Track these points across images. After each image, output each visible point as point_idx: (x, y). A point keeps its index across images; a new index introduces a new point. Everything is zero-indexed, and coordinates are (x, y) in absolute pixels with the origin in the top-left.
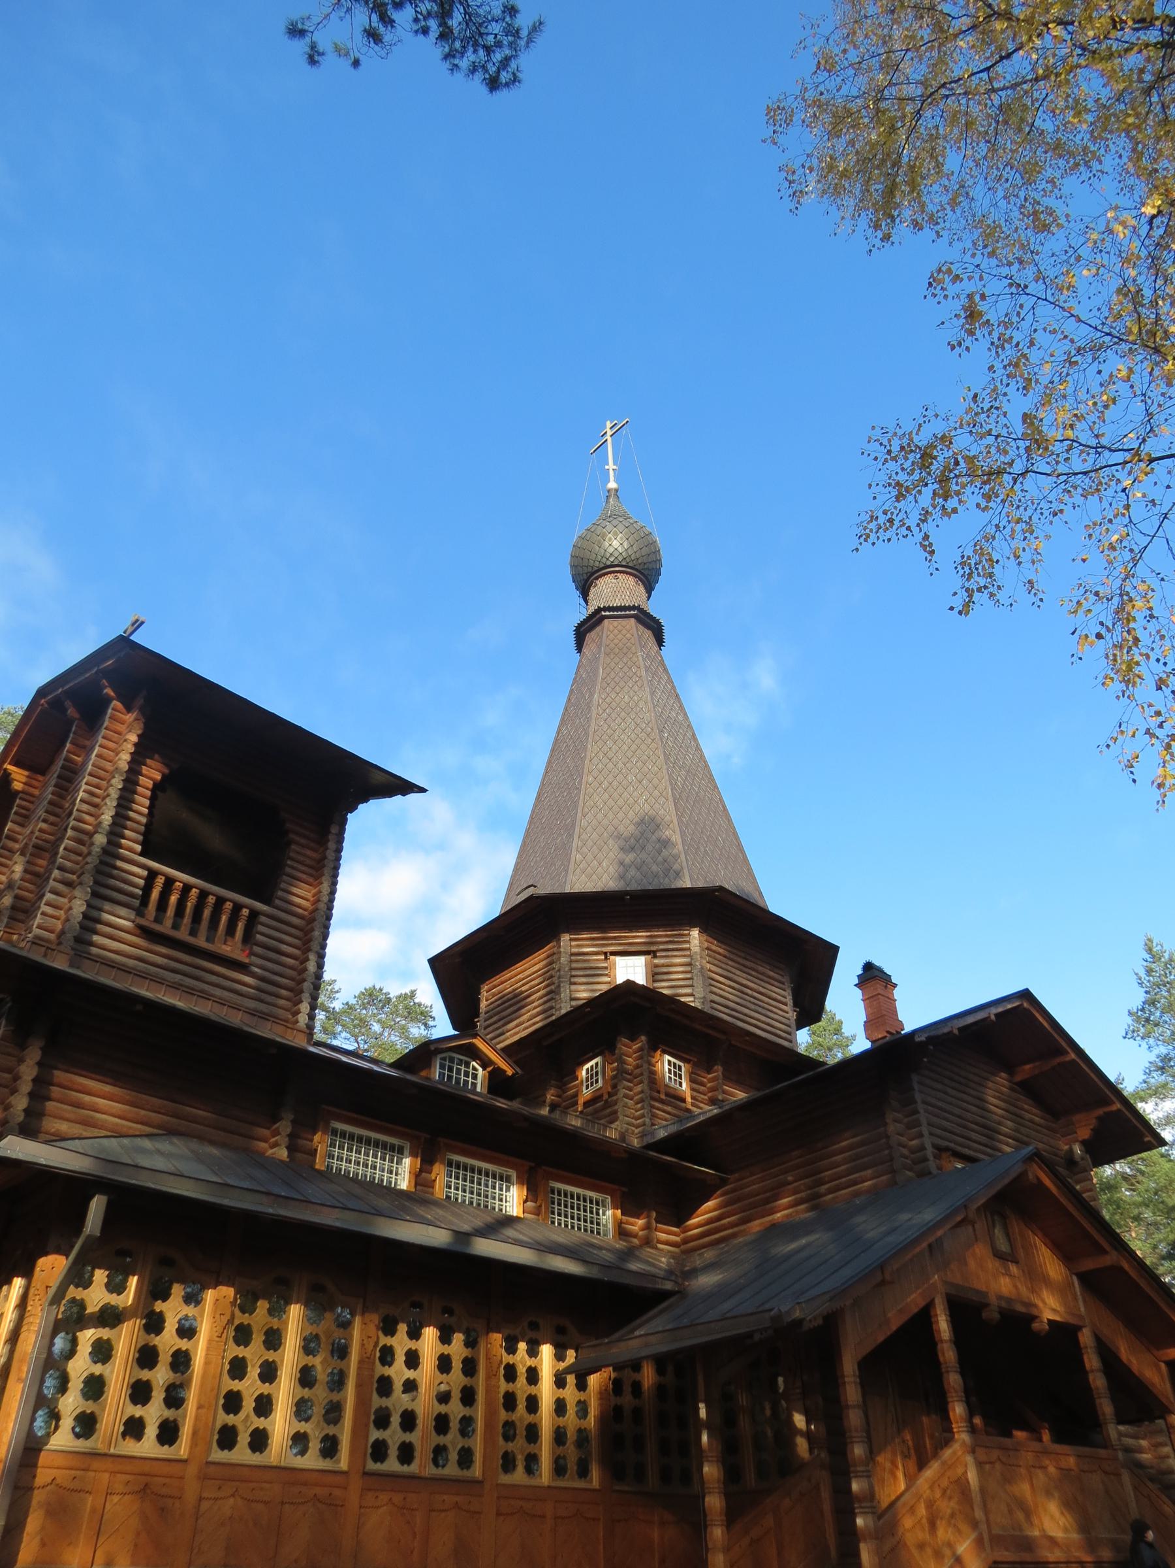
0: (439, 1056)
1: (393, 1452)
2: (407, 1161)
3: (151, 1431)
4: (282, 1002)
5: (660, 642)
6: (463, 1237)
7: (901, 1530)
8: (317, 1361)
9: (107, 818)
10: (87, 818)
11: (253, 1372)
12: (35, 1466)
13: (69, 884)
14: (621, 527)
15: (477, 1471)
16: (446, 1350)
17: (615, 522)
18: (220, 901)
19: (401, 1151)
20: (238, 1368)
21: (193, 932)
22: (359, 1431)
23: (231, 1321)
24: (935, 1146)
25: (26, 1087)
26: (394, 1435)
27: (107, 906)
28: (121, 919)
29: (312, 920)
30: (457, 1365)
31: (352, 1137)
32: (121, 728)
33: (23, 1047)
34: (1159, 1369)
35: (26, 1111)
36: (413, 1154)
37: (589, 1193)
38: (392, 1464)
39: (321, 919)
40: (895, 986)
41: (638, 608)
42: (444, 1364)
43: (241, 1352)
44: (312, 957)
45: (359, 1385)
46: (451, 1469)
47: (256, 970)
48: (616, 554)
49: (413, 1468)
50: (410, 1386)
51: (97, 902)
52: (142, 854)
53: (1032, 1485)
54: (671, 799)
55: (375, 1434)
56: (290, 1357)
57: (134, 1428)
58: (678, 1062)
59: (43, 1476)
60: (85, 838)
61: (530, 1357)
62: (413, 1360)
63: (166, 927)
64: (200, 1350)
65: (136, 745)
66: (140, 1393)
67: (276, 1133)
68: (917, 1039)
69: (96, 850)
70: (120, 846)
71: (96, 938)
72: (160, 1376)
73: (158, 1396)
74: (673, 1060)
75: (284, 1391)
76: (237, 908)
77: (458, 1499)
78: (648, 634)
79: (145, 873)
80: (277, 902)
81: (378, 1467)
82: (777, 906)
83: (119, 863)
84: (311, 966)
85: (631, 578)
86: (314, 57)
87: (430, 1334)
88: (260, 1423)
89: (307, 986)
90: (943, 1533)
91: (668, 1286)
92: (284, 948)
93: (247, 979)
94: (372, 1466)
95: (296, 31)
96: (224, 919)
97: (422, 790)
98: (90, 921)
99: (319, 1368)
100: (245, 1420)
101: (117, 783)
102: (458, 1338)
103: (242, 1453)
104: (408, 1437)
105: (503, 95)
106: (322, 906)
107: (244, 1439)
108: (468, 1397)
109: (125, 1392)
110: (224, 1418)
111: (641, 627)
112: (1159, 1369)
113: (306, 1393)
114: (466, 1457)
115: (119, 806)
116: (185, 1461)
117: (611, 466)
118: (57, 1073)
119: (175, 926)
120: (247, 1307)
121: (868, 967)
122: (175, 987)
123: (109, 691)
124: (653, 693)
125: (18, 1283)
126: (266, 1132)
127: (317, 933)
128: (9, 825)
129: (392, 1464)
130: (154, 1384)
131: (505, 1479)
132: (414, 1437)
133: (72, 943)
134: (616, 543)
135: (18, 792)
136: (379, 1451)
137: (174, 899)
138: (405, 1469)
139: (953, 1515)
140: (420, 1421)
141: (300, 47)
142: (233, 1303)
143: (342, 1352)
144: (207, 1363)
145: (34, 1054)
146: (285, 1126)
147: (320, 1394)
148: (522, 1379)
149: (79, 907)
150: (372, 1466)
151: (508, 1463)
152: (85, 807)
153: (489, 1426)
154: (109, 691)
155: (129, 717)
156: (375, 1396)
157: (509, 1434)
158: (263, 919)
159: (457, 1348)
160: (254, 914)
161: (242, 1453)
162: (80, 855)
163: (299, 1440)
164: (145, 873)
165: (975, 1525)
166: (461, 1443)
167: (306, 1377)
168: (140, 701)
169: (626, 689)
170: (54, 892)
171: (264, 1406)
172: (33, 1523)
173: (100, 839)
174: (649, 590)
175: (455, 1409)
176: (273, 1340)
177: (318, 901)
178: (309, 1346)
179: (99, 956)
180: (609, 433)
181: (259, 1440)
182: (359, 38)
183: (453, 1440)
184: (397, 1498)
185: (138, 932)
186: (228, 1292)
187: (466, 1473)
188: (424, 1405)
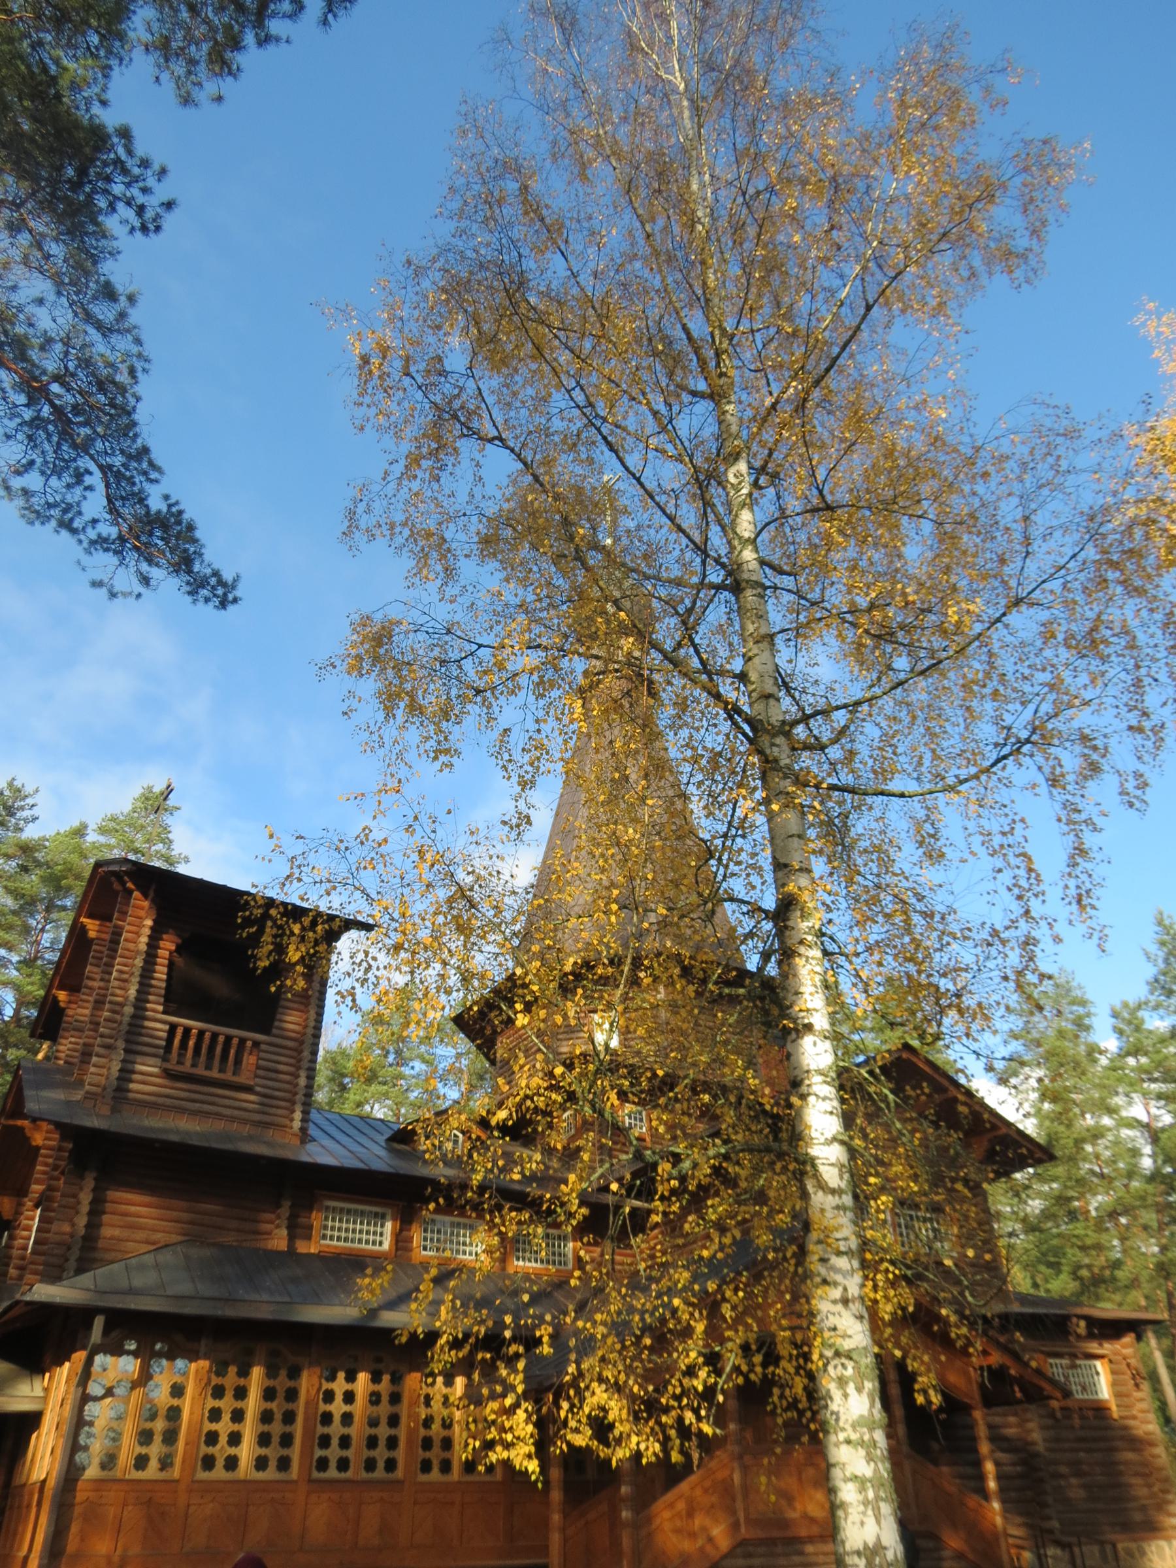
1: (333, 1464)
2: (389, 1225)
4: (280, 1112)
6: (373, 1313)
7: (657, 1521)
8: (273, 1406)
9: (132, 992)
10: (118, 992)
11: (226, 1417)
12: (75, 1490)
13: (108, 1047)
15: (399, 1473)
16: (376, 1388)
19: (383, 1217)
20: (215, 1415)
21: (208, 1067)
22: (306, 1452)
25: (85, 1208)
26: (334, 1453)
27: (139, 1059)
28: (148, 1067)
29: (302, 1043)
30: (385, 1398)
31: (342, 1210)
32: (142, 913)
33: (82, 1177)
34: (966, 1374)
35: (87, 1226)
36: (394, 1219)
38: (332, 1473)
39: (309, 1040)
42: (375, 1399)
43: (217, 1403)
44: (303, 1074)
45: (306, 1419)
46: (380, 1473)
47: (258, 1089)
49: (349, 1474)
50: (347, 1418)
51: (131, 1057)
52: (164, 1012)
53: (800, 1479)
55: (319, 1453)
56: (253, 1403)
59: (80, 1496)
60: (117, 1008)
62: (349, 1397)
63: (187, 1067)
65: (152, 928)
67: (279, 1217)
69: (126, 1019)
70: (146, 1010)
71: (132, 1086)
72: (159, 1425)
73: (158, 1438)
75: (249, 1430)
80: (274, 1031)
81: (322, 1475)
83: (147, 1023)
84: (302, 1081)
86: (113, 595)
87: (363, 1377)
88: (232, 1451)
89: (300, 1097)
90: (698, 1521)
92: (281, 1067)
93: (252, 1098)
94: (316, 1475)
95: (97, 584)
96: (232, 1052)
98: (126, 1073)
99: (275, 1410)
100: (221, 1450)
101: (139, 962)
102: (386, 1378)
103: (219, 1473)
104: (345, 1453)
105: (231, 608)
106: (310, 1031)
107: (220, 1463)
108: (394, 1421)
110: (205, 1450)
112: (966, 1374)
113: (266, 1428)
114: (391, 1465)
115: (142, 976)
118: (109, 1193)
119: (194, 1065)
120: (221, 1372)
122: (194, 1113)
125: (67, 1364)
126: (272, 1216)
127: (306, 1054)
128: (89, 968)
129: (332, 1473)
131: (423, 1478)
132: (349, 1453)
135: (93, 940)
136: (323, 1464)
137: (191, 1043)
138: (343, 1475)
139: (712, 1506)
140: (354, 1442)
141: (103, 591)
142: (210, 1371)
143: (292, 1395)
144: (191, 1413)
145: (89, 1183)
146: (285, 1211)
147: (277, 1428)
149: (116, 1067)
150: (316, 1475)
151: (426, 1466)
152: (117, 983)
153: (410, 1441)
155: (146, 904)
156: (319, 1426)
157: (427, 1443)
159: (385, 1386)
161: (219, 1473)
162: (115, 1022)
163: (261, 1463)
164: (167, 1027)
165: (733, 1512)
166: (387, 1454)
167: (266, 1417)
168: (151, 894)
170: (98, 1055)
171: (235, 1439)
172: (74, 1529)
173: (129, 1010)
175: (383, 1431)
176: (241, 1393)
177: (306, 1027)
178: (269, 1394)
179: (135, 1100)
181: (232, 1463)
182: (135, 581)
183: (381, 1454)
186: (204, 1364)
187: (391, 1476)
188: (356, 1431)
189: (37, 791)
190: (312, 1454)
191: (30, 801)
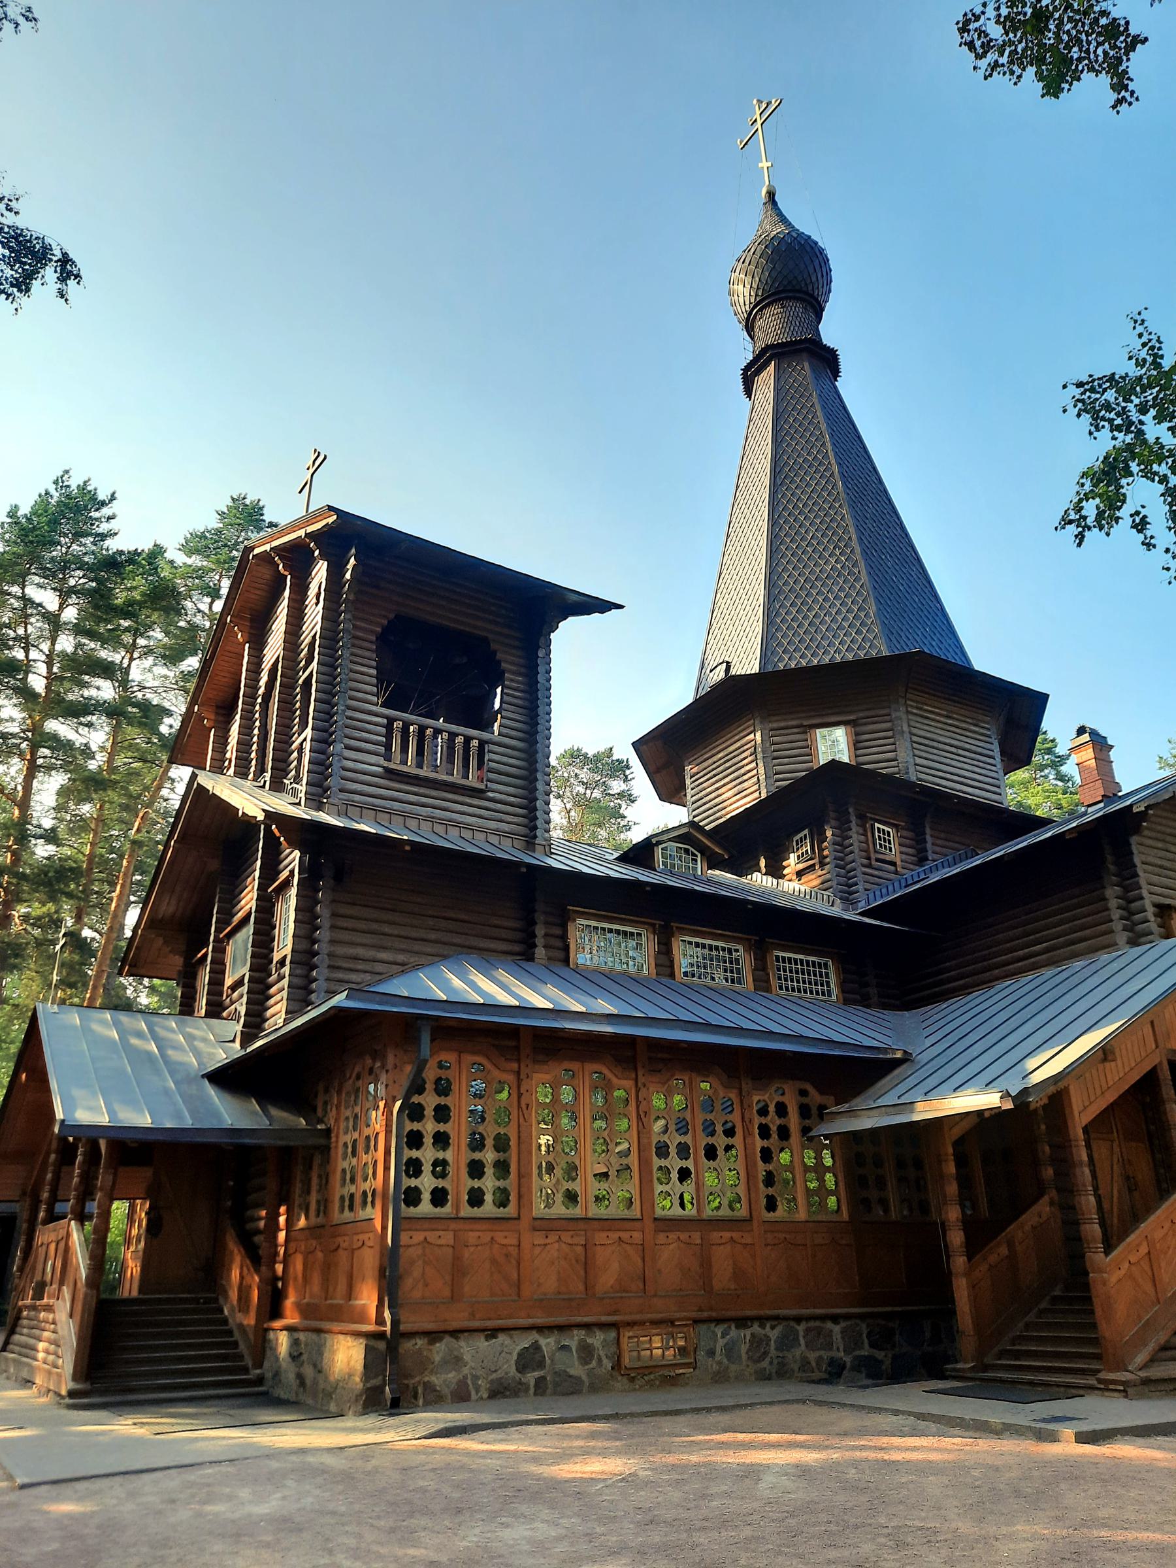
0: (660, 847)
24: (1156, 905)
37: (811, 958)
40: (1112, 747)
57: (476, 1199)
58: (887, 829)
61: (780, 1117)
66: (476, 1170)
68: (1135, 810)
72: (489, 1156)
73: (489, 1171)
74: (880, 826)
76: (468, 740)
77: (734, 1235)
79: (385, 721)
91: (899, 1055)
116: (518, 1218)
131: (771, 1216)
148: (775, 1136)
156: (655, 1158)
158: (492, 747)
160: (482, 743)
164: (385, 721)
184: (684, 1236)
189: (113, 498)
191: (105, 511)
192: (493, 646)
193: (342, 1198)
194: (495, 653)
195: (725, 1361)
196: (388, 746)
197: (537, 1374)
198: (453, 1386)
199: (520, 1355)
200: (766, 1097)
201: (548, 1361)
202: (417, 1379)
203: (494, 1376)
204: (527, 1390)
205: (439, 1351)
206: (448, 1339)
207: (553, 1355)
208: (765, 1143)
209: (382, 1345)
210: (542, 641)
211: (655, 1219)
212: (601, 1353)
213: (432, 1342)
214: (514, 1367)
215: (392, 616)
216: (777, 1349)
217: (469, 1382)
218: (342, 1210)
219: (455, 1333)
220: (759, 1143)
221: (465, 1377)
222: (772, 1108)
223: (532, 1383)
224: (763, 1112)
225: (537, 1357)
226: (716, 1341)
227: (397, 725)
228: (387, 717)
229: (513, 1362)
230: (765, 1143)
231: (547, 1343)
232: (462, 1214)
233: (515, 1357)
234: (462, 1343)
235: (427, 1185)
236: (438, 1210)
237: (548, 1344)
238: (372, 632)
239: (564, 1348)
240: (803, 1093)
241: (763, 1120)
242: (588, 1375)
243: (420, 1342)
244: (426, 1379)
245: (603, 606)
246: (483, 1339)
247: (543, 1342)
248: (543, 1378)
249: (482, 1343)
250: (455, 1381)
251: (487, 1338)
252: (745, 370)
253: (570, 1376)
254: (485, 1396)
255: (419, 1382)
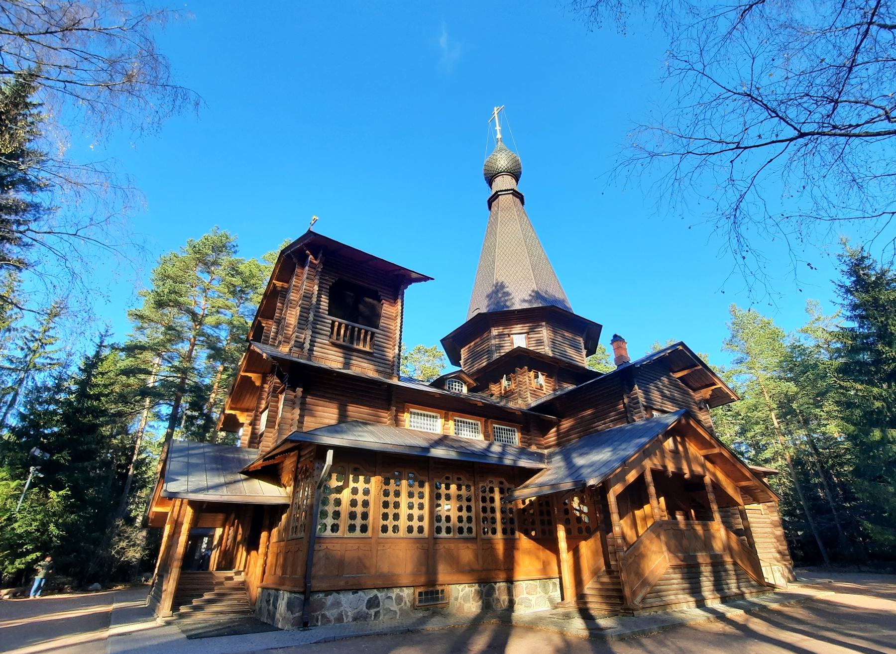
3: (358, 529)
5: (523, 203)
14: (503, 155)
17: (501, 153)
18: (360, 330)
23: (381, 488)
31: (418, 414)
40: (626, 343)
41: (513, 190)
46: (465, 534)
48: (502, 167)
51: (314, 335)
52: (328, 315)
54: (531, 270)
63: (341, 342)
64: (371, 498)
75: (404, 511)
78: (518, 200)
82: (576, 312)
85: (509, 177)
88: (396, 523)
97: (433, 279)
102: (464, 487)
107: (390, 529)
109: (347, 516)
111: (514, 198)
117: (498, 128)
120: (387, 483)
121: (615, 336)
123: (307, 252)
124: (521, 226)
130: (357, 512)
133: (307, 351)
134: (502, 162)
140: (452, 519)
154: (307, 252)
158: (376, 335)
164: (331, 322)
166: (468, 525)
169: (510, 225)
174: (517, 181)
180: (496, 112)
181: (396, 529)
185: (331, 344)
190: (434, 525)
192: (380, 293)
193: (293, 527)
194: (380, 296)
195: (462, 602)
196: (332, 333)
197: (376, 610)
198: (336, 615)
199: (369, 601)
200: (485, 485)
201: (381, 604)
202: (319, 613)
203: (356, 611)
204: (371, 617)
205: (330, 599)
206: (335, 594)
207: (384, 600)
208: (484, 505)
209: (302, 597)
210: (400, 292)
211: (434, 538)
212: (407, 600)
213: (326, 595)
214: (365, 607)
215: (337, 279)
216: (485, 596)
217: (343, 613)
218: (292, 534)
219: (338, 591)
220: (481, 505)
221: (342, 612)
222: (487, 489)
223: (373, 614)
224: (484, 491)
225: (376, 602)
226: (459, 593)
227: (337, 323)
228: (332, 321)
229: (365, 604)
230: (484, 505)
231: (381, 595)
232: (345, 536)
233: (366, 602)
234: (341, 596)
235: (329, 523)
236: (334, 534)
237: (381, 596)
238: (328, 285)
239: (390, 598)
240: (501, 483)
241: (484, 495)
242: (399, 610)
243: (321, 595)
244: (323, 613)
245: (426, 279)
246: (351, 593)
247: (379, 595)
248: (379, 612)
249: (350, 596)
250: (336, 613)
251: (353, 593)
252: (489, 201)
253: (392, 611)
254: (351, 620)
255: (319, 614)
